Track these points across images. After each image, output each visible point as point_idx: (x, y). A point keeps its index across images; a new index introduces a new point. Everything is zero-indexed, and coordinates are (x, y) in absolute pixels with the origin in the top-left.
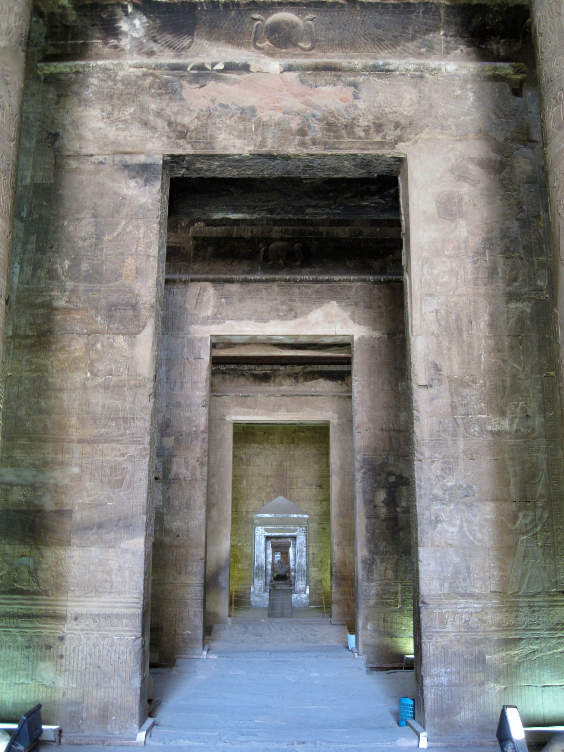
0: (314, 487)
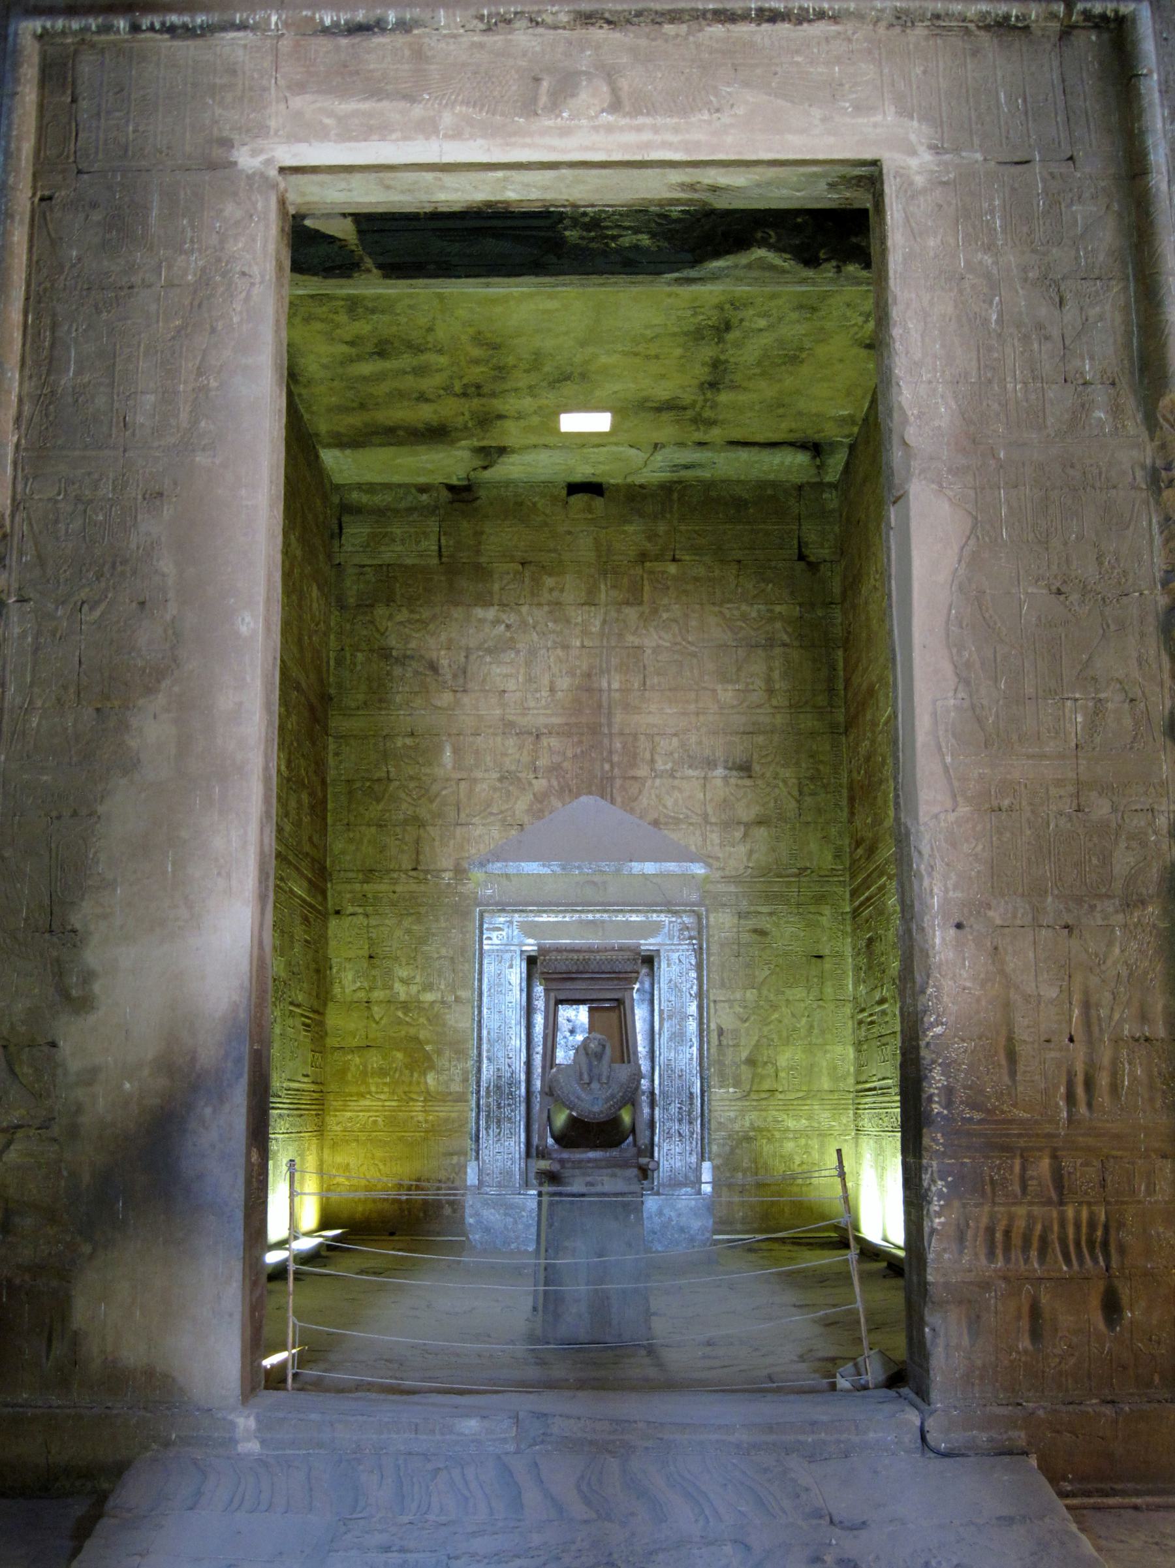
0: (720, 771)
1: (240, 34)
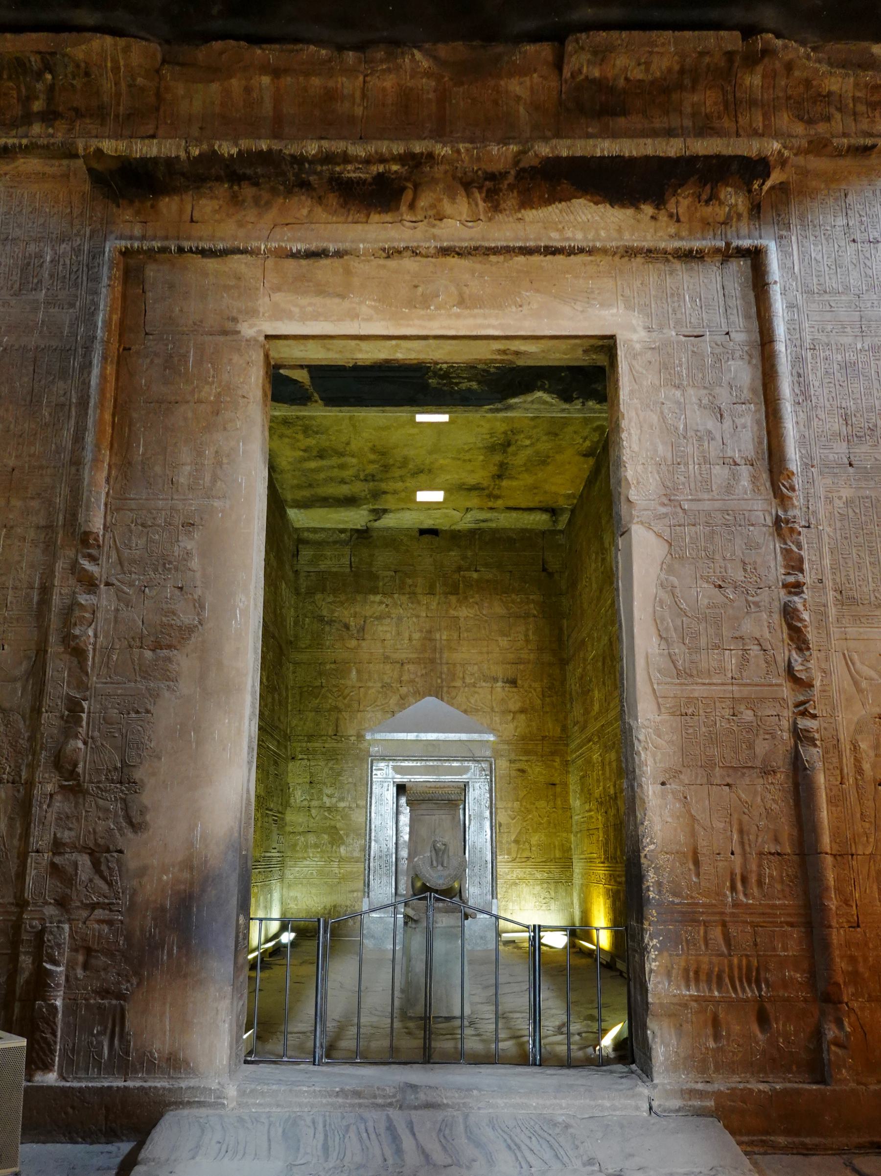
0: (500, 684)
1: (244, 256)
